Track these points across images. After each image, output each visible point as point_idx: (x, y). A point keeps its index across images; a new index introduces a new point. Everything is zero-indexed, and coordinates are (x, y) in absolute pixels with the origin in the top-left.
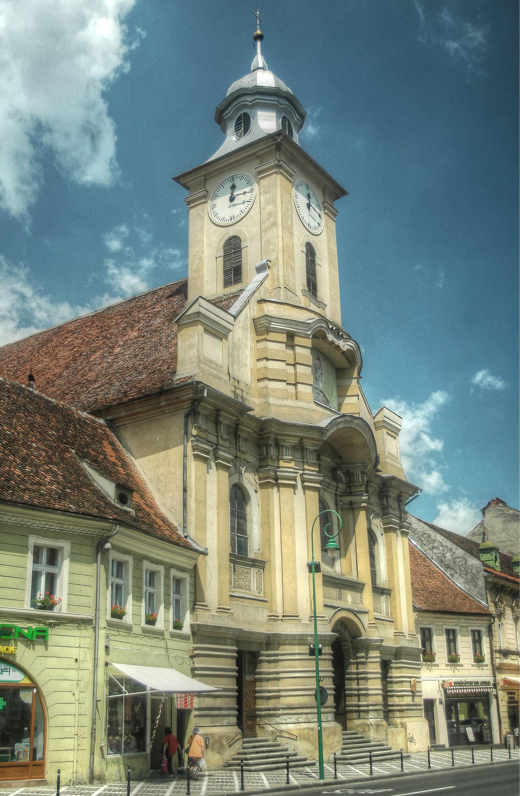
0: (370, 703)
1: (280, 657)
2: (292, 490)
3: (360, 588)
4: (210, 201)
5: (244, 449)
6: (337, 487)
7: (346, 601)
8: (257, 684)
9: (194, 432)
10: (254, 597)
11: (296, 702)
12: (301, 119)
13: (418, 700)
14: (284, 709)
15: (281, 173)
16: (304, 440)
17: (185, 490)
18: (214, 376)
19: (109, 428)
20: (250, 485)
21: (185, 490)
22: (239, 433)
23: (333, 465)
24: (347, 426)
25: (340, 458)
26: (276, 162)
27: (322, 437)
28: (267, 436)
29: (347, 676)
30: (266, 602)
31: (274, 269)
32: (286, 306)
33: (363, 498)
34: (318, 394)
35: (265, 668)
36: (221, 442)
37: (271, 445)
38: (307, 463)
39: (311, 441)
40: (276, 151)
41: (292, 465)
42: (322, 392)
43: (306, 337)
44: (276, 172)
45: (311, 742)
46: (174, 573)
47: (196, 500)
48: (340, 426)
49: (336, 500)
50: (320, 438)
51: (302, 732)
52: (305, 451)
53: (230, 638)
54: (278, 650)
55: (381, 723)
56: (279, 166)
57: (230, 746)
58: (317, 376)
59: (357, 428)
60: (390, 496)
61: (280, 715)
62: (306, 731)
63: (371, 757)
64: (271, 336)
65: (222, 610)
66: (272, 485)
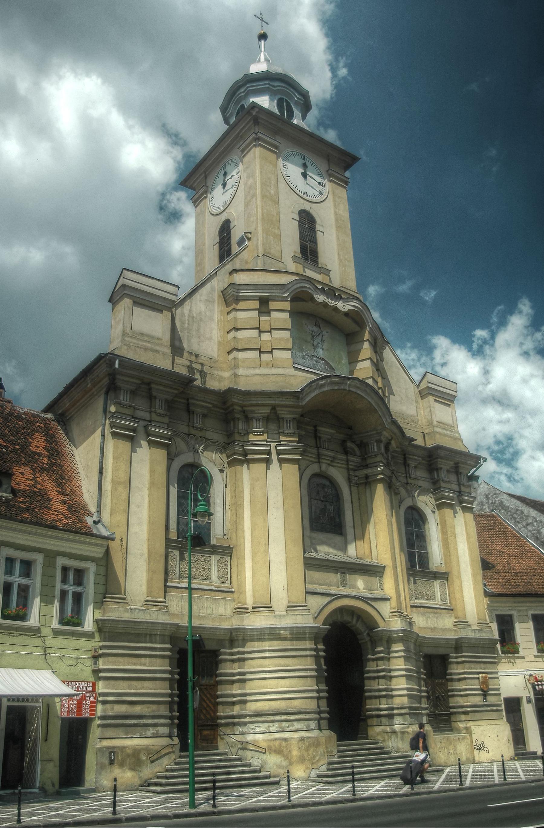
0: (395, 706)
1: (246, 656)
2: (264, 465)
3: (379, 572)
4: (209, 195)
5: (198, 425)
6: (347, 461)
7: (354, 587)
8: (219, 687)
9: (113, 409)
10: (213, 588)
11: (267, 708)
12: (304, 98)
13: (491, 699)
14: (251, 716)
15: (260, 145)
16: (278, 409)
17: (101, 472)
18: (146, 349)
19: (58, 422)
20: (212, 465)
21: (101, 472)
22: (192, 408)
23: (341, 436)
24: (336, 388)
25: (350, 428)
26: (254, 135)
27: (298, 402)
28: (231, 408)
29: (366, 675)
30: (233, 592)
31: (254, 239)
32: (260, 273)
33: (379, 469)
34: (317, 361)
35: (226, 669)
36: (154, 417)
37: (238, 419)
38: (284, 433)
39: (287, 409)
40: (255, 125)
41: (265, 437)
42: (323, 359)
43: (284, 300)
44: (255, 146)
45: (284, 756)
46: (61, 561)
47: (112, 481)
48: (326, 389)
49: (349, 475)
50: (296, 404)
51: (272, 743)
52: (281, 420)
53: (160, 635)
54: (244, 647)
55: (406, 730)
56: (258, 139)
57: (152, 762)
58: (315, 343)
59: (351, 389)
60: (441, 468)
61: (245, 724)
62: (277, 743)
63: (353, 774)
64: (242, 305)
65: (149, 603)
66: (241, 463)
